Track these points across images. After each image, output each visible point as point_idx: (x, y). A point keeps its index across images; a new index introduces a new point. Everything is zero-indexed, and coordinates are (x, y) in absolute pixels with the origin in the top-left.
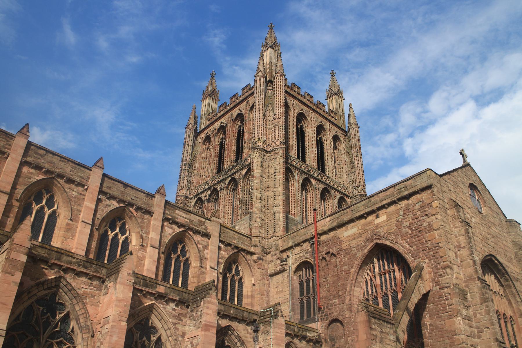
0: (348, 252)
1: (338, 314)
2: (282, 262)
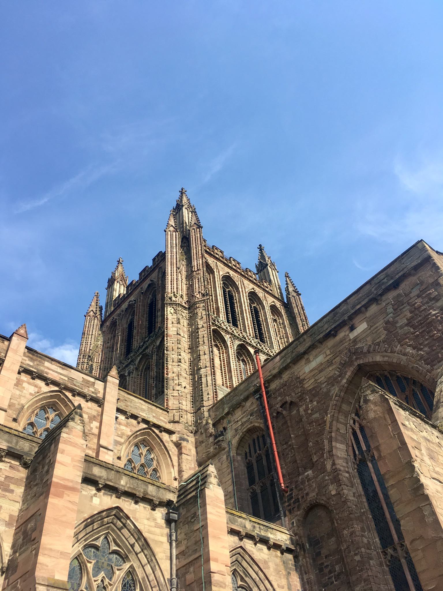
0: (315, 392)
1: (317, 494)
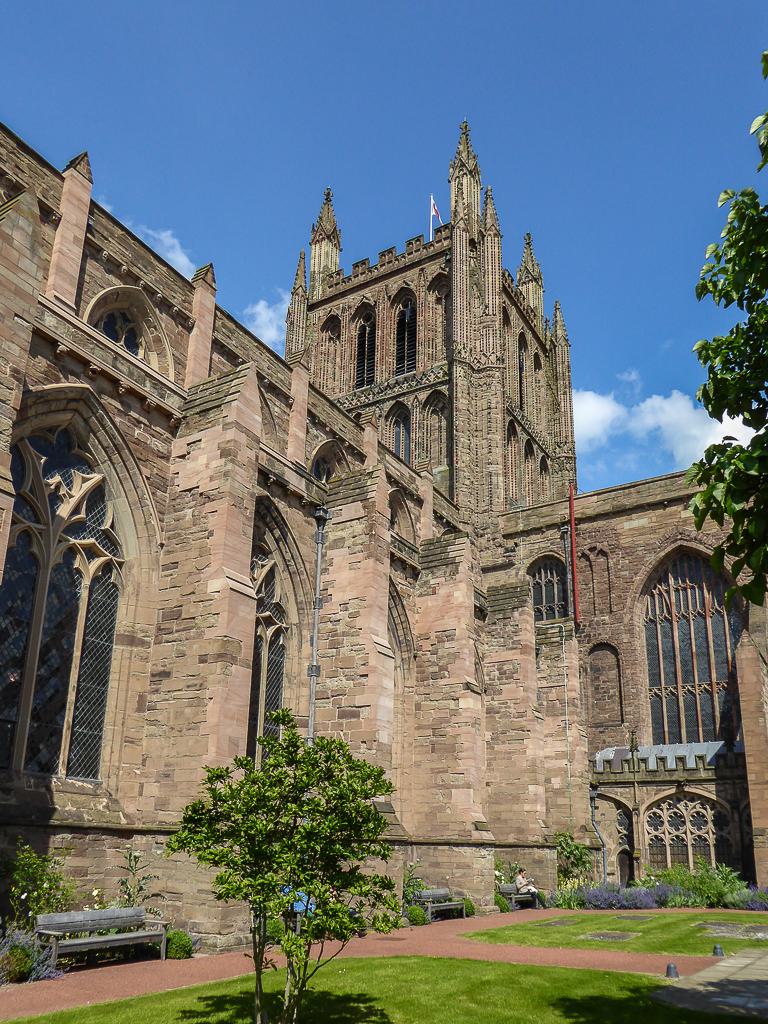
2: (507, 550)
